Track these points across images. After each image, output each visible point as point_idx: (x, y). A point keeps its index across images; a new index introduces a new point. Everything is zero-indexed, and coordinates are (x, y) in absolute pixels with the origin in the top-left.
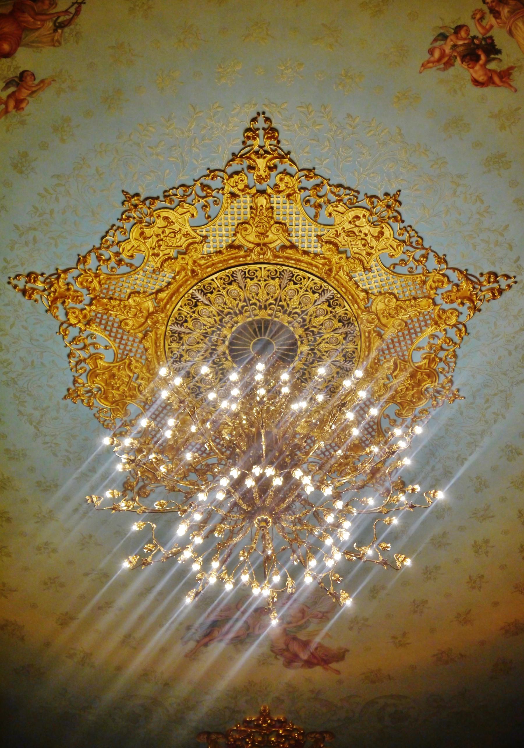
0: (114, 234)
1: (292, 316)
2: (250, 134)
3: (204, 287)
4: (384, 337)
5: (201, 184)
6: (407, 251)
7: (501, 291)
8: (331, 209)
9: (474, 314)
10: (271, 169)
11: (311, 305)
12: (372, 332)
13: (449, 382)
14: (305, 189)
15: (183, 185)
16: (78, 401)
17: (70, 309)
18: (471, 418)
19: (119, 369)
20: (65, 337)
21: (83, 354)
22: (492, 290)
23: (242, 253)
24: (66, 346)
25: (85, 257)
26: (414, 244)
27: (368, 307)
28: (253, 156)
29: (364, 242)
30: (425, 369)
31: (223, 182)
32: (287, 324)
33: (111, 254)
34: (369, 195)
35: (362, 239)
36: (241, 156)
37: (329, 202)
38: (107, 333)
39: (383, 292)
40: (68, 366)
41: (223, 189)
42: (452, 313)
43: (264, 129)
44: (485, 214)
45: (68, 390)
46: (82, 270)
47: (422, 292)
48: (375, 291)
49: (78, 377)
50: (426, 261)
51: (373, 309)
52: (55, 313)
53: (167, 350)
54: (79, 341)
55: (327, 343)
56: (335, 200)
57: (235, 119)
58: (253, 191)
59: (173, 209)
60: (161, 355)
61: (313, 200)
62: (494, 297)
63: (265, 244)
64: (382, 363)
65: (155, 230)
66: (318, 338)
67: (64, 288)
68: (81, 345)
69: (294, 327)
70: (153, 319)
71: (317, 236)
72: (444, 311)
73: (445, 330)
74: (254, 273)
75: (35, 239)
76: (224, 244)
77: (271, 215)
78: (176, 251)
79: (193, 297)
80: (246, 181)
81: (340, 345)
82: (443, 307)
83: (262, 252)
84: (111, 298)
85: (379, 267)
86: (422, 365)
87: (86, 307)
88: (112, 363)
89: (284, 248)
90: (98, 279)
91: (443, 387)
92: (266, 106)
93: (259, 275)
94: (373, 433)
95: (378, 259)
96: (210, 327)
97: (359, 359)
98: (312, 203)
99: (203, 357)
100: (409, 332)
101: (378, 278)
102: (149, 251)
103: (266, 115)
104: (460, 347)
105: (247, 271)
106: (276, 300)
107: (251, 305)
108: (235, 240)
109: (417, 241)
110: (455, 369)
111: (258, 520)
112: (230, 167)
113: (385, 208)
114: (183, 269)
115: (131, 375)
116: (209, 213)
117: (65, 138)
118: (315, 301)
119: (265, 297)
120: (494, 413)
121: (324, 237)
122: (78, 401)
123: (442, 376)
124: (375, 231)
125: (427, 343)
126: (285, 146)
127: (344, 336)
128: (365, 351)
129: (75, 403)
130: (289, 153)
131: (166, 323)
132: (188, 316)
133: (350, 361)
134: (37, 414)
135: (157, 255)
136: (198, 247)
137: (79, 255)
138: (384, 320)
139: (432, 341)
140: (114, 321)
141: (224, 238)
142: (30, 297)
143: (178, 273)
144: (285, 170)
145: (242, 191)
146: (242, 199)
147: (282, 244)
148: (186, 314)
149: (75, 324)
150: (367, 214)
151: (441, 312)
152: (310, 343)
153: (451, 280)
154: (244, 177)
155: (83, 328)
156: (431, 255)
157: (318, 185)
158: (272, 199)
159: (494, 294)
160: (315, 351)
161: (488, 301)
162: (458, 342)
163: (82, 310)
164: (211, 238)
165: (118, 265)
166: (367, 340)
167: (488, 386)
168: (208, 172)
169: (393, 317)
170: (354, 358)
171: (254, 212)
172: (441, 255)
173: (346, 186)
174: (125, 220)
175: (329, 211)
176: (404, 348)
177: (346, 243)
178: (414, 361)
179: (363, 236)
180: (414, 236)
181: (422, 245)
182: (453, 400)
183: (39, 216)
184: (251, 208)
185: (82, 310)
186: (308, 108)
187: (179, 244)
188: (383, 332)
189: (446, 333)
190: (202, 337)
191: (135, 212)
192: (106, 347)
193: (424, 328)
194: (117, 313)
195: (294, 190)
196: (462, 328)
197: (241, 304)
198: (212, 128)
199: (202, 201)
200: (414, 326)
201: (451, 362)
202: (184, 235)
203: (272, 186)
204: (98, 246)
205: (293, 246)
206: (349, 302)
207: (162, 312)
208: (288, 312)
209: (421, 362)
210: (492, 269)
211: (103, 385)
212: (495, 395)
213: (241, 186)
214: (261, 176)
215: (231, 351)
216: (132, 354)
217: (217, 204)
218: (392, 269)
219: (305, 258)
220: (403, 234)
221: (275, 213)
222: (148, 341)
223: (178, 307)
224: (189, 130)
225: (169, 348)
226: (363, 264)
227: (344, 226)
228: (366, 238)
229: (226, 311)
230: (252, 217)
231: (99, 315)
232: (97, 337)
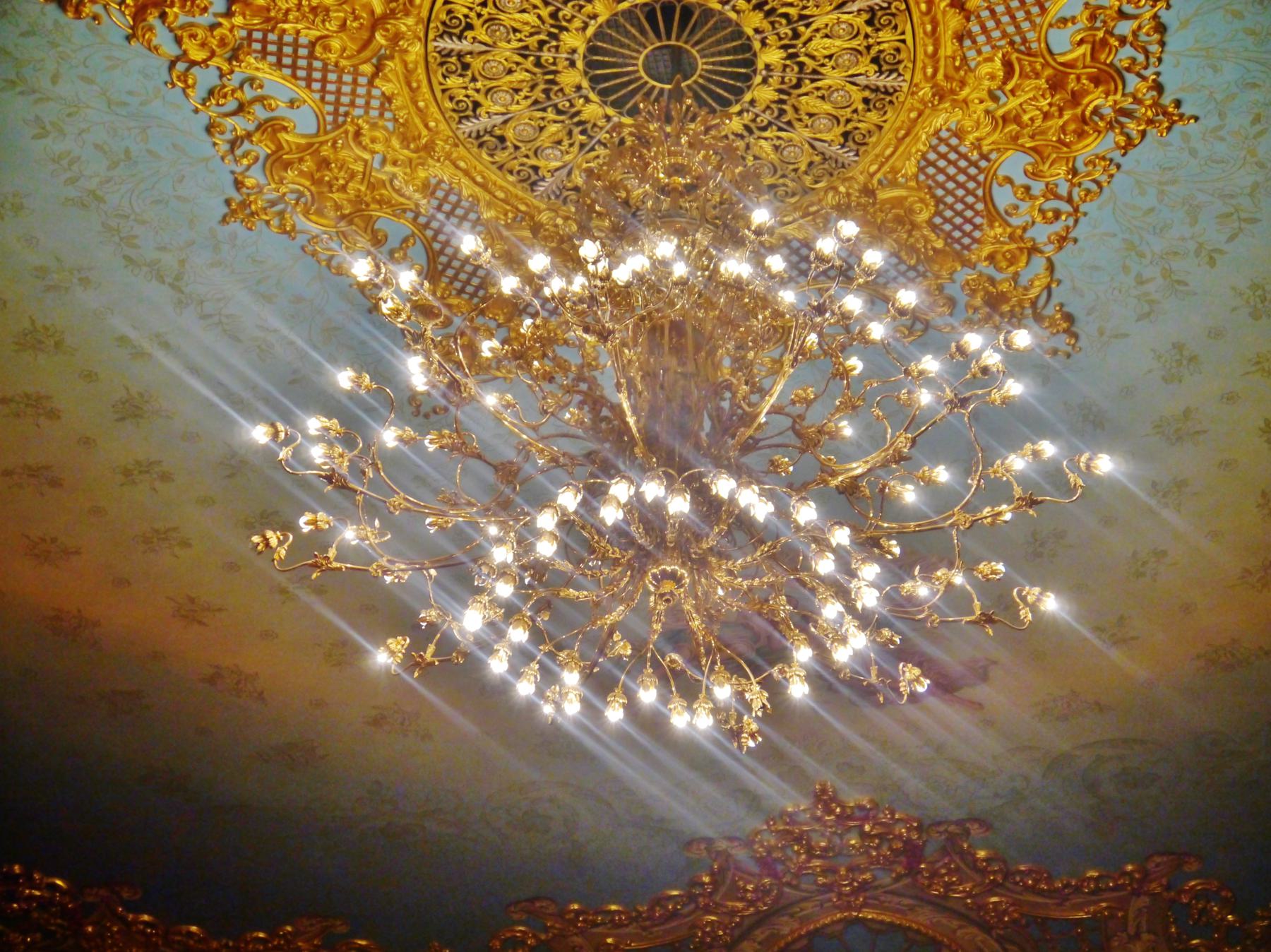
13: (1150, 88)
16: (260, 225)
17: (182, 27)
18: (1217, 162)
20: (189, 91)
21: (240, 125)
24: (196, 111)
30: (1085, 67)
38: (287, 72)
40: (212, 151)
45: (228, 202)
49: (242, 173)
52: (149, 41)
53: (439, 94)
54: (225, 96)
55: (827, 36)
60: (427, 106)
64: (973, 64)
66: (802, 29)
68: (232, 105)
69: (738, 12)
70: (387, 30)
81: (861, 37)
86: (1076, 60)
87: (221, 20)
91: (1138, 101)
94: (978, 220)
96: (532, 35)
97: (914, 62)
99: (529, 101)
110: (1164, 56)
111: (654, 576)
115: (367, 156)
122: (260, 225)
125: (1082, 8)
127: (865, 16)
128: (925, 45)
129: (250, 229)
131: (422, 35)
132: (472, 14)
133: (891, 72)
140: (296, 45)
142: (78, 13)
148: (466, 11)
149: (205, 61)
155: (225, 67)
163: (213, 27)
166: (927, 19)
167: (1254, 85)
170: (900, 62)
176: (1025, 26)
178: (1055, 50)
185: (213, 27)
190: (518, 59)
192: (292, 103)
194: (299, 26)
201: (1150, 43)
207: (407, 14)
209: (1071, 51)
211: (308, 183)
215: (594, 80)
216: (358, 112)
222: (389, 81)
225: (444, 91)
229: (532, 42)
231: (257, 35)
232: (266, 84)
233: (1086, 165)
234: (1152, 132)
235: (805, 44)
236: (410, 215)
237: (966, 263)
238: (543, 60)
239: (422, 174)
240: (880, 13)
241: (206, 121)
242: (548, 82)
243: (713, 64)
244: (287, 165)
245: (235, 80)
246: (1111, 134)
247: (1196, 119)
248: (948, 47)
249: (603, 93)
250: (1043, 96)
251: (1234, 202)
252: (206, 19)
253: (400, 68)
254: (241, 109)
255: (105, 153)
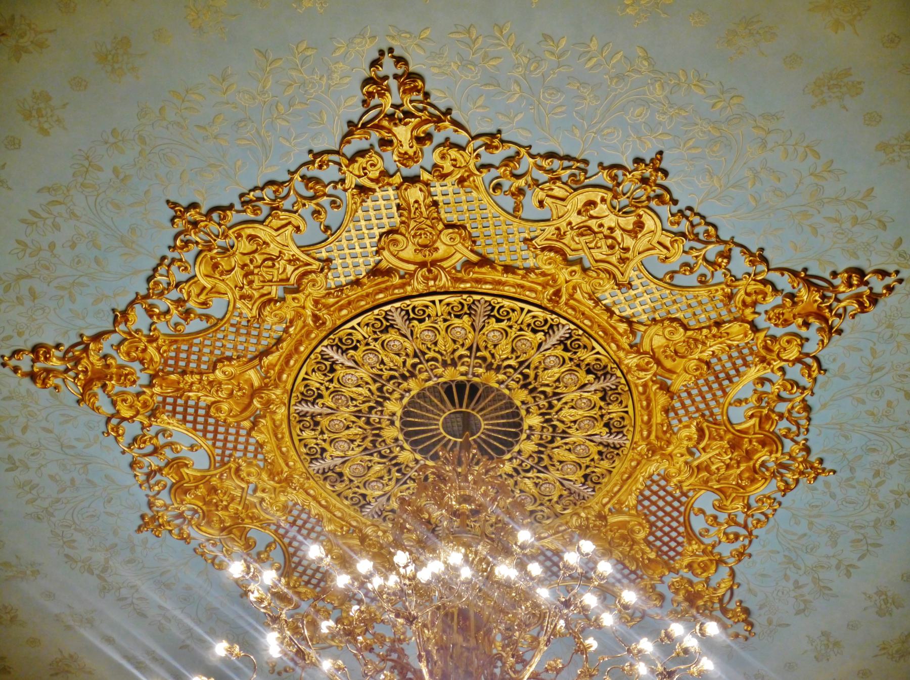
0: (168, 271)
1: (502, 371)
2: (372, 88)
3: (340, 340)
4: (672, 389)
5: (303, 177)
6: (692, 248)
7: (874, 299)
8: (542, 195)
9: (829, 339)
10: (420, 140)
11: (533, 352)
12: (650, 384)
13: (801, 450)
14: (488, 166)
15: (271, 183)
17: (117, 394)
19: (220, 478)
20: (119, 438)
21: (154, 462)
22: (858, 298)
23: (396, 280)
24: (124, 452)
25: (124, 313)
26: (701, 237)
27: (636, 345)
28: (385, 123)
29: (610, 241)
30: (755, 434)
31: (340, 170)
32: (496, 386)
33: (168, 303)
34: (605, 164)
35: (606, 237)
36: (364, 126)
37: (536, 183)
38: (190, 425)
39: (658, 318)
40: (133, 480)
41: (343, 181)
42: (788, 342)
43: (396, 77)
44: (825, 174)
45: (143, 517)
46: (124, 332)
47: (730, 311)
48: (644, 318)
49: (154, 496)
50: (728, 263)
51: (646, 347)
52: (93, 404)
53: (297, 443)
54: (144, 442)
55: (572, 407)
56: (546, 179)
57: (341, 65)
58: (397, 179)
59: (262, 222)
60: (288, 451)
61: (506, 183)
62: (863, 309)
63: (434, 263)
64: (676, 429)
65: (237, 259)
66: (555, 402)
67: (99, 365)
68: (149, 448)
69: (510, 389)
71: (525, 240)
72: (774, 338)
73: (782, 369)
74: (424, 312)
75: (32, 292)
76: (363, 270)
77: (435, 215)
78: (281, 289)
79: (325, 357)
80: (380, 165)
81: (597, 409)
82: (771, 332)
83: (431, 276)
84: (184, 373)
85: (645, 279)
86: (749, 428)
87: (145, 389)
88: (208, 470)
89: (468, 265)
90: (155, 345)
92: (393, 37)
93: (433, 313)
94: (680, 539)
95: (642, 268)
96: (364, 402)
97: (634, 427)
98: (506, 188)
99: (361, 449)
100: (717, 377)
101: (646, 297)
102: (233, 293)
103: (396, 53)
104: (813, 394)
105: (410, 308)
106: (470, 349)
107: (428, 361)
108: (380, 261)
109: (707, 231)
110: (810, 427)
112: (347, 146)
113: (639, 184)
114: (299, 315)
115: (244, 485)
116: (326, 223)
117: (46, 126)
118: (540, 345)
119: (450, 346)
120: (892, 492)
121: (538, 240)
122: (164, 533)
123: (787, 442)
124: (628, 222)
125: (752, 393)
126: (440, 100)
127: (600, 394)
128: (642, 415)
129: (158, 536)
130: (449, 111)
131: (286, 401)
132: (323, 388)
133: (618, 433)
134: (99, 557)
135: (250, 297)
136: (318, 279)
137: (114, 310)
138: (668, 364)
139: (759, 387)
140: (197, 407)
141: (361, 260)
142: (44, 384)
143: (291, 322)
144: (447, 139)
145: (376, 181)
146: (379, 194)
147: (464, 259)
148: (318, 385)
149: (132, 418)
150: (609, 196)
151: (769, 342)
152: (544, 411)
153: (779, 287)
154: (375, 158)
155: (146, 422)
156: (736, 251)
157: (510, 159)
158: (432, 189)
159: (861, 304)
160: (555, 423)
161: (853, 316)
162: (809, 385)
163: (139, 394)
164: (337, 262)
165: (186, 320)
167: (874, 450)
168: (310, 157)
169: (683, 357)
170: (624, 427)
171: (405, 213)
172: (754, 250)
173: (562, 154)
174: (182, 248)
175: (540, 197)
176: (713, 404)
177: (579, 246)
178: (734, 421)
179: (607, 232)
180: (699, 224)
181: (717, 237)
182: (815, 478)
183: (31, 255)
184: (399, 207)
185: (139, 394)
186: (469, 32)
187: (283, 276)
188: (669, 382)
189: (784, 373)
191: (195, 233)
192: (192, 447)
193: (742, 369)
194: (200, 394)
195: (470, 171)
196: (814, 364)
197: (410, 361)
198: (304, 84)
199: (311, 206)
200: (723, 366)
201: (800, 418)
202: (289, 261)
203: (429, 168)
204: (143, 292)
205: (485, 261)
206: (601, 341)
207: (276, 387)
208: (494, 367)
209: (745, 422)
210: (853, 263)
211: (200, 504)
212: (891, 462)
213: (374, 174)
214: (406, 153)
215: (407, 435)
217: (339, 207)
218: (669, 280)
219: (509, 278)
220: (678, 223)
221: (442, 211)
222: (262, 433)
223: (302, 375)
224: (263, 93)
225: (300, 440)
226: (614, 278)
227: (571, 219)
228: (613, 235)
229: (365, 407)
230: (402, 222)
232: (174, 433)
233: (757, 502)
234: (803, 480)
235: (557, 412)
236: (273, 527)
237: (672, 570)
238: (371, 420)
239: (282, 498)
240: (610, 393)
241: (130, 459)
242: (375, 435)
243: (492, 425)
244: (186, 491)
245: (152, 431)
246: (774, 481)
247: (835, 472)
248: (658, 417)
249: (414, 444)
250: (725, 452)
251: (862, 531)
252: (134, 389)
253: (270, 424)
254: (156, 451)
255: (57, 481)
